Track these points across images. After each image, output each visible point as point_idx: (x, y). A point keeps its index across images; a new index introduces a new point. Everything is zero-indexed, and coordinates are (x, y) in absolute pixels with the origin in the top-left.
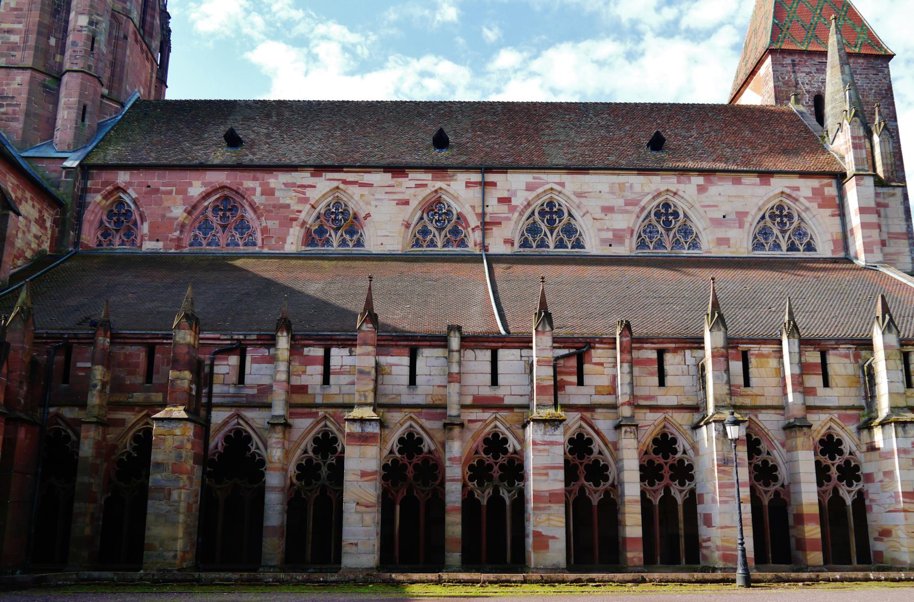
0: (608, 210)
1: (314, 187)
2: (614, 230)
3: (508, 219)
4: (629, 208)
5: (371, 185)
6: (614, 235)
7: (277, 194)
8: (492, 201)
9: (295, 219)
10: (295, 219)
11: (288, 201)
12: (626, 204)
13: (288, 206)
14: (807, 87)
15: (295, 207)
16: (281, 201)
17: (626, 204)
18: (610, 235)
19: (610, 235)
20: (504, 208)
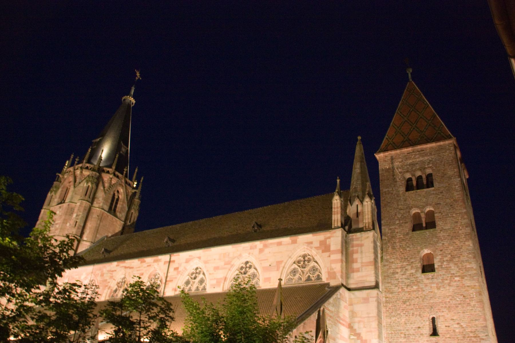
0: (216, 268)
1: (115, 271)
2: (217, 279)
3: (176, 278)
4: (226, 266)
5: (132, 268)
6: (217, 282)
7: (105, 275)
8: (171, 270)
9: (107, 286)
10: (107, 286)
11: (107, 278)
12: (225, 264)
13: (106, 280)
14: (400, 170)
15: (108, 281)
16: (105, 278)
17: (225, 264)
18: (214, 282)
19: (214, 282)
20: (176, 272)
